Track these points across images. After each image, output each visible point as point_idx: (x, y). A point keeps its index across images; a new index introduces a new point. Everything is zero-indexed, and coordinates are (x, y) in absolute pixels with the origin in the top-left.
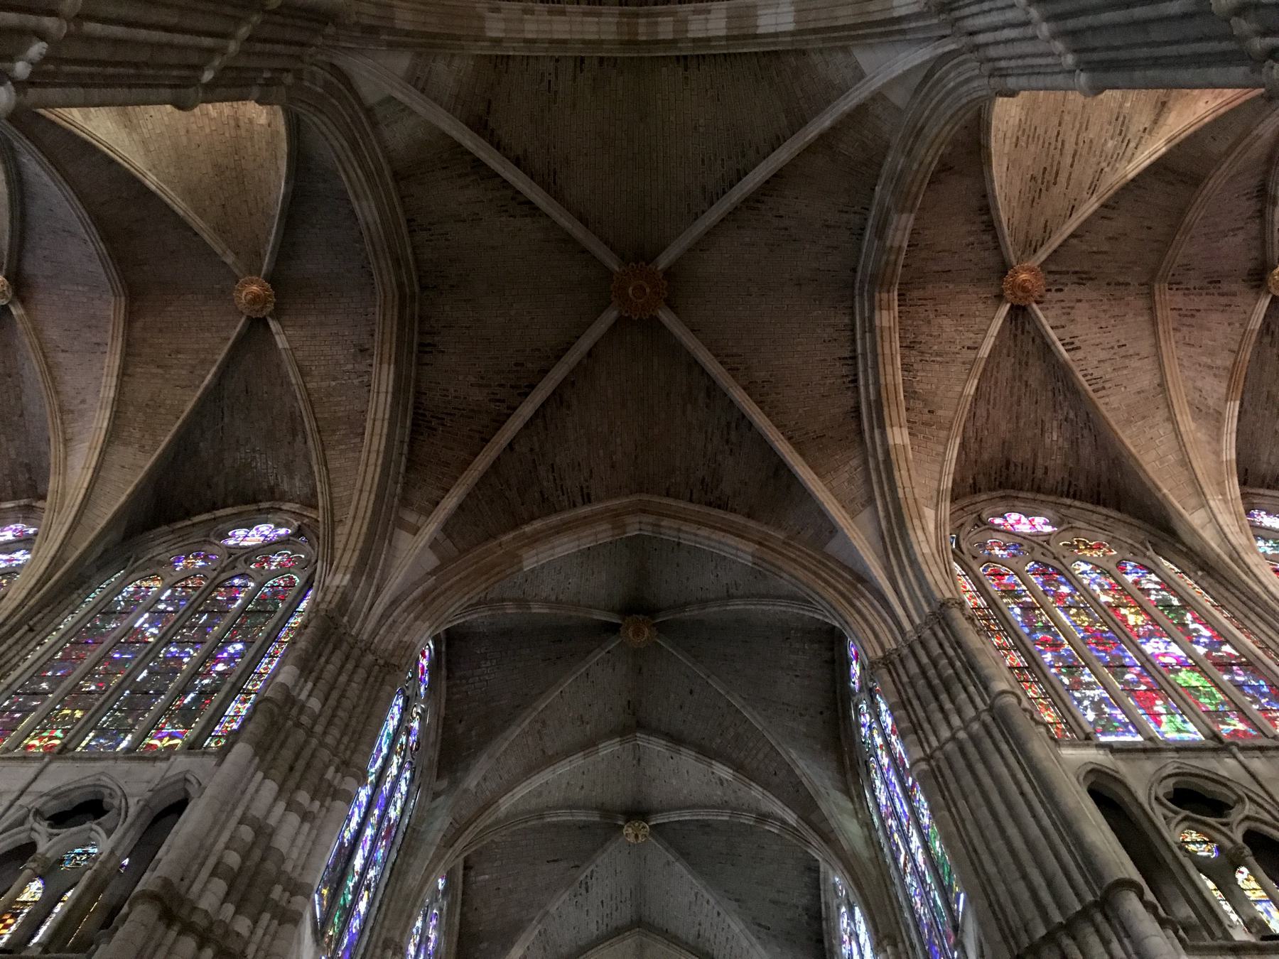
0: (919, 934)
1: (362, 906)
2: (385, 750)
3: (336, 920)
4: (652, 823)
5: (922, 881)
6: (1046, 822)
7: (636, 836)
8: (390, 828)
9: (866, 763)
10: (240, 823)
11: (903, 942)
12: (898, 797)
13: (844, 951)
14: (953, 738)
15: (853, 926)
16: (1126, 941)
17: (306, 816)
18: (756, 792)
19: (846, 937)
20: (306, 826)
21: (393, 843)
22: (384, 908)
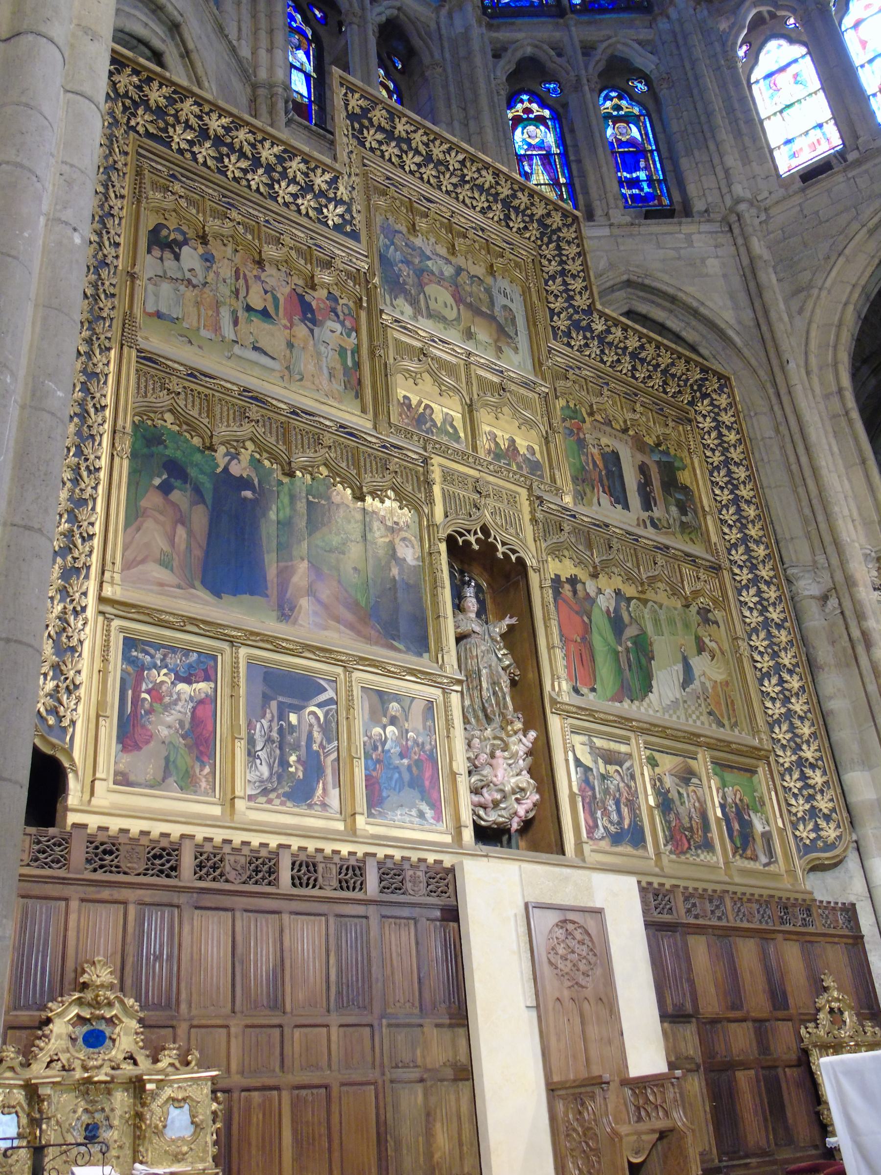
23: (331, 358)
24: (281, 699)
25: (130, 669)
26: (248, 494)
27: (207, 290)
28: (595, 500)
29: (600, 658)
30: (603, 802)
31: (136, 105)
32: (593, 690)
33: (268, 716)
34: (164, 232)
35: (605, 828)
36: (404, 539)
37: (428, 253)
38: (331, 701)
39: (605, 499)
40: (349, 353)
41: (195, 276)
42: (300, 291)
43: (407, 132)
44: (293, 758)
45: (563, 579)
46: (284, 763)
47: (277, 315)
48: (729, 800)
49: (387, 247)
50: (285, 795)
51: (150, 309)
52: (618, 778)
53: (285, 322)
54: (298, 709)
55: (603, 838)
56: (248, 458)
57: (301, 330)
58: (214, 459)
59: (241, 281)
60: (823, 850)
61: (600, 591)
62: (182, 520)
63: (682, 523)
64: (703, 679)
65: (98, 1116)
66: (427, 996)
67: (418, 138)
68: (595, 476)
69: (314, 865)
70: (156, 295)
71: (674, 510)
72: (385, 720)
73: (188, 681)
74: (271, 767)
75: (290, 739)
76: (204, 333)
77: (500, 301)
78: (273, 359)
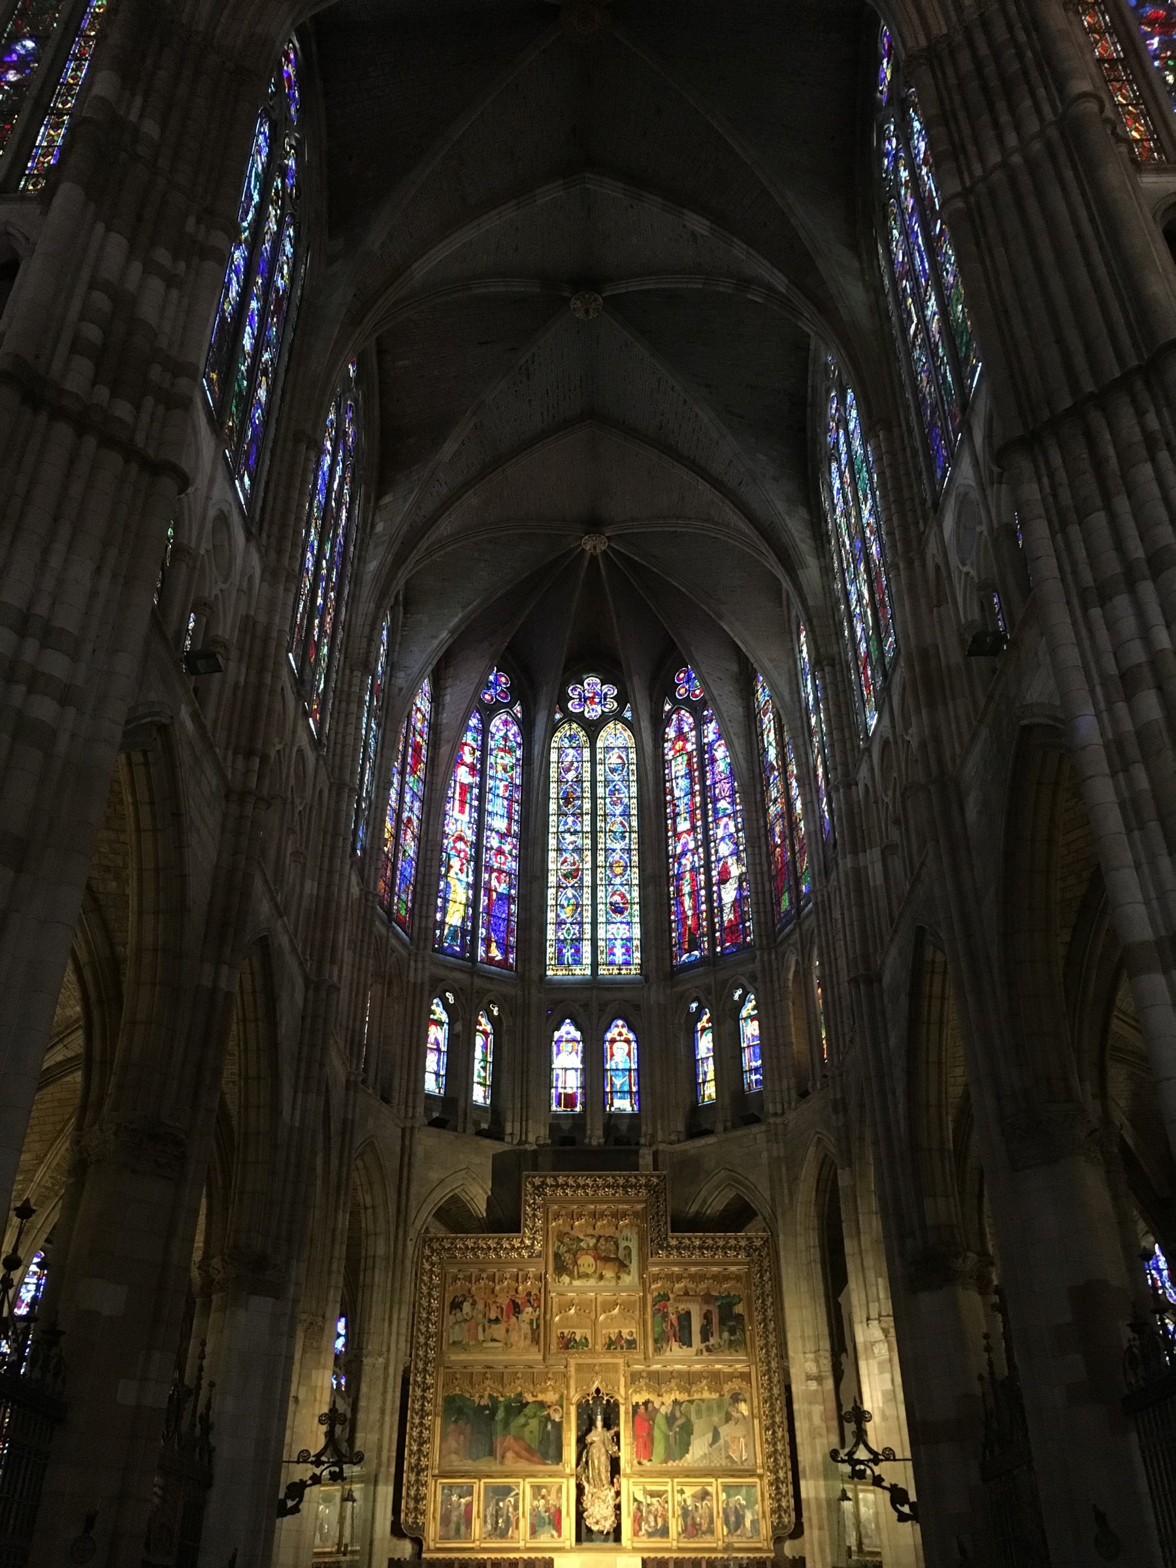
0: (920, 415)
1: (262, 394)
2: (256, 198)
3: (234, 409)
4: (604, 295)
5: (933, 354)
6: (1102, 271)
7: (587, 312)
8: (279, 300)
9: (885, 206)
10: (92, 286)
11: (900, 426)
12: (919, 251)
13: (829, 439)
14: (1004, 164)
15: (842, 412)
16: (1165, 411)
17: (171, 281)
18: (739, 249)
19: (833, 424)
20: (174, 294)
21: (286, 320)
22: (288, 397)
23: (526, 1328)
26: (487, 1412)
29: (656, 1443)
30: (647, 1518)
32: (650, 1460)
35: (646, 1530)
37: (582, 1237)
39: (675, 1346)
44: (500, 1521)
46: (497, 1523)
48: (731, 1505)
49: (559, 1247)
51: (451, 1342)
54: (503, 1500)
57: (514, 1319)
61: (663, 1404)
63: (730, 1341)
67: (571, 1182)
68: (671, 1333)
71: (726, 1335)
77: (623, 1244)
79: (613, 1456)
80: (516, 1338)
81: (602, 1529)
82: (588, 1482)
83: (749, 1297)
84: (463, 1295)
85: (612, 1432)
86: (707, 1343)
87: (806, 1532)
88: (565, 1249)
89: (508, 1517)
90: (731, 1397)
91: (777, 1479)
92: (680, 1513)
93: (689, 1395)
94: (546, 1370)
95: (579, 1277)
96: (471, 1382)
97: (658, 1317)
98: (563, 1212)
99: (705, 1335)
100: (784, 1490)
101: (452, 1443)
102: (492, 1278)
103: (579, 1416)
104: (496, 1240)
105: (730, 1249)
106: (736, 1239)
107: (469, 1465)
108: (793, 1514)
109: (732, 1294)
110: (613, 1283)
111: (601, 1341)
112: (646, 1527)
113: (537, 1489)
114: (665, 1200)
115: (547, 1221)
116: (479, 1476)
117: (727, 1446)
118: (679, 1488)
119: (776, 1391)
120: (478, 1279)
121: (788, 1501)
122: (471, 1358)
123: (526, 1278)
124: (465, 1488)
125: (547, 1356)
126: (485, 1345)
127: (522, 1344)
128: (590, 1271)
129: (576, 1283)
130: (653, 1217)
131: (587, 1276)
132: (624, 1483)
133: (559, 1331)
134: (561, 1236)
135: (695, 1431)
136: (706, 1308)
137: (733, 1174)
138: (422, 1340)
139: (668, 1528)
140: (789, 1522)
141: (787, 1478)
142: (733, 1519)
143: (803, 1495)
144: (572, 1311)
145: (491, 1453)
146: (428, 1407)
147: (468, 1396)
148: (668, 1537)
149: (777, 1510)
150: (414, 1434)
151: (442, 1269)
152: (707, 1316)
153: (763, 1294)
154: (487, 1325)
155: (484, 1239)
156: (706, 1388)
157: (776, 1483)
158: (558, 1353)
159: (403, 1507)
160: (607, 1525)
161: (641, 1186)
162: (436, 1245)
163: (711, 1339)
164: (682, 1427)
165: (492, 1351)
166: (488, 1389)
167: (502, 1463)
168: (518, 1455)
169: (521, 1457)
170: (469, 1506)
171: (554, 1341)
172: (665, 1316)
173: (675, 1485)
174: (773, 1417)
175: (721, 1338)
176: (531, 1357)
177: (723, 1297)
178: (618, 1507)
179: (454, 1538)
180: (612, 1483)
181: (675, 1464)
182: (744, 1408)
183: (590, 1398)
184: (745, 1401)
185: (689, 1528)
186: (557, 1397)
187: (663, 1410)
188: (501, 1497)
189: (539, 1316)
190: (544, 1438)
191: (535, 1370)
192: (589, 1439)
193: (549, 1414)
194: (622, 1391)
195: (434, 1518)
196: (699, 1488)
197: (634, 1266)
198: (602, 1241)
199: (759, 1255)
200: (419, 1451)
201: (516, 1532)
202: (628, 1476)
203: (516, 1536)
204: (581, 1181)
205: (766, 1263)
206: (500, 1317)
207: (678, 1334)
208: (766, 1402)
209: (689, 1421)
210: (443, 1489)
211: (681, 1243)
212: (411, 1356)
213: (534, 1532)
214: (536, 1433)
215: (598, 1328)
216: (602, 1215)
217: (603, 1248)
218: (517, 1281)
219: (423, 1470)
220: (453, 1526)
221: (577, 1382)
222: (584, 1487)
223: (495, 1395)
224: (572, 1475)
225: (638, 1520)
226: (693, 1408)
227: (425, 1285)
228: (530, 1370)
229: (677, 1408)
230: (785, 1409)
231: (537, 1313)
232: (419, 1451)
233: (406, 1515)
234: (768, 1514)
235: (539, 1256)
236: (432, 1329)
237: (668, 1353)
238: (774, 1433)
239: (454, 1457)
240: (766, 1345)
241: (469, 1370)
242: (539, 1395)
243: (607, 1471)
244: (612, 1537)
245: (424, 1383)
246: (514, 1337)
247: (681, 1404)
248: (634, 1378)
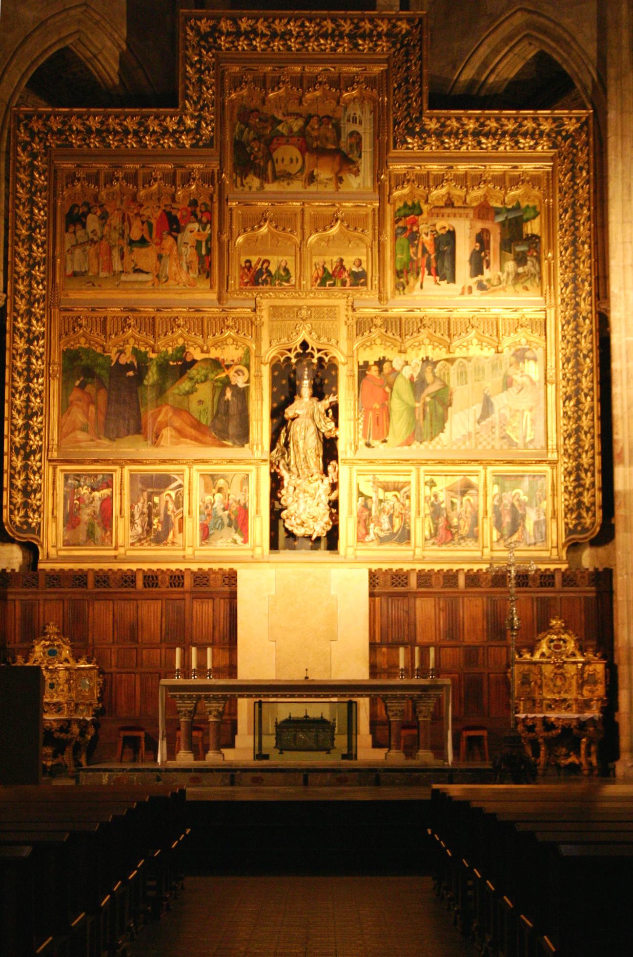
23: (189, 253)
24: (150, 490)
25: (68, 490)
26: (131, 373)
27: (104, 242)
28: (418, 285)
29: (394, 418)
30: (378, 518)
31: (47, 134)
32: (385, 441)
33: (142, 501)
34: (76, 211)
35: (375, 534)
36: (236, 372)
38: (181, 486)
39: (429, 280)
40: (204, 244)
41: (96, 235)
42: (168, 209)
43: (251, 26)
44: (155, 521)
45: (371, 363)
46: (150, 524)
47: (151, 238)
48: (505, 501)
49: (242, 132)
50: (150, 540)
51: (69, 271)
52: (395, 499)
53: (157, 240)
54: (158, 494)
55: (372, 541)
56: (131, 349)
57: (169, 241)
58: (110, 357)
59: (126, 223)
60: (581, 533)
62: (92, 402)
64: (503, 411)
65: (54, 681)
66: (217, 634)
67: (261, 27)
69: (157, 577)
70: (72, 261)
71: (510, 265)
72: (214, 491)
73: (98, 490)
74: (143, 527)
75: (154, 511)
76: (103, 274)
77: (349, 128)
78: (147, 273)
79: (328, 435)
80: (174, 268)
81: (310, 533)
82: (289, 470)
83: (550, 211)
84: (86, 204)
85: (326, 403)
86: (480, 277)
87: (621, 536)
88: (252, 135)
89: (167, 517)
90: (514, 355)
91: (579, 467)
92: (428, 511)
93: (449, 352)
94: (223, 315)
95: (276, 178)
96: (104, 331)
97: (403, 240)
98: (250, 77)
99: (478, 265)
100: (588, 482)
101: (78, 416)
102: (132, 178)
103: (274, 381)
104: (136, 119)
105: (525, 135)
106: (535, 119)
107: (105, 448)
108: (599, 514)
109: (524, 204)
110: (331, 188)
111: (310, 273)
112: (377, 530)
113: (211, 479)
114: (420, 58)
115: (221, 92)
116: (121, 463)
117: (504, 423)
118: (428, 478)
119: (585, 345)
120: (110, 179)
121: (594, 496)
122: (101, 296)
123: (187, 179)
124: (100, 477)
125: (225, 295)
126: (123, 278)
127: (184, 277)
128: (294, 168)
129: (270, 187)
130: (400, 86)
131: (288, 177)
132: (343, 471)
133: (243, 259)
134: (245, 115)
135: (454, 402)
136: (479, 225)
137: (535, 17)
138: (22, 269)
139: (409, 532)
140: (593, 524)
141: (593, 464)
142: (507, 519)
143: (620, 484)
144: (264, 230)
145: (139, 429)
146: (38, 365)
147: (99, 350)
148: (409, 543)
149: (577, 508)
150: (18, 402)
151: (50, 163)
152: (482, 239)
153: (574, 204)
154: (126, 249)
155: (117, 117)
156: (475, 341)
157: (576, 472)
158: (241, 290)
159: (5, 501)
160: (320, 528)
161: (379, 36)
162: (37, 126)
163: (486, 271)
164: (435, 396)
165: (137, 286)
166: (132, 341)
167: (156, 443)
168: (180, 433)
169: (186, 437)
170: (107, 503)
171: (235, 273)
172: (414, 237)
173: (422, 474)
174: (579, 381)
175: (501, 269)
176: (198, 296)
177: (508, 210)
178: (334, 504)
179: (86, 543)
180: (325, 472)
181: (422, 447)
182: (533, 370)
183: (292, 355)
184: (535, 360)
185: (442, 532)
186: (240, 353)
187: (407, 372)
188: (155, 490)
189: (210, 235)
190: (222, 411)
191: (206, 315)
192: (289, 412)
193: (227, 377)
194: (344, 345)
195: (55, 517)
196: (458, 479)
197: (366, 162)
198: (314, 123)
199: (572, 145)
200: (27, 427)
201: (179, 536)
202: (351, 463)
203: (179, 538)
204: (279, 26)
205: (582, 156)
206: (147, 237)
207: (433, 265)
208: (568, 360)
209: (445, 386)
210: (66, 478)
211: (443, 126)
212: (5, 291)
213: (206, 534)
214: (209, 404)
215: (306, 253)
216: (314, 82)
217: (315, 133)
218: (174, 183)
219: (34, 452)
220: (83, 528)
221: (271, 331)
222: (282, 479)
223: (143, 349)
224: (265, 460)
225: (364, 522)
226: (453, 369)
227: (23, 186)
228: (197, 315)
229: (429, 369)
230: (596, 370)
231: (208, 231)
232: (27, 427)
233: (11, 512)
234: (561, 514)
235: (209, 145)
236: (38, 253)
237: (417, 292)
238: (578, 402)
239: (81, 435)
240: (574, 279)
241: (101, 314)
242: (213, 350)
243: (318, 456)
244: (323, 544)
245: (29, 331)
246: (171, 267)
247: (435, 364)
248: (362, 326)
